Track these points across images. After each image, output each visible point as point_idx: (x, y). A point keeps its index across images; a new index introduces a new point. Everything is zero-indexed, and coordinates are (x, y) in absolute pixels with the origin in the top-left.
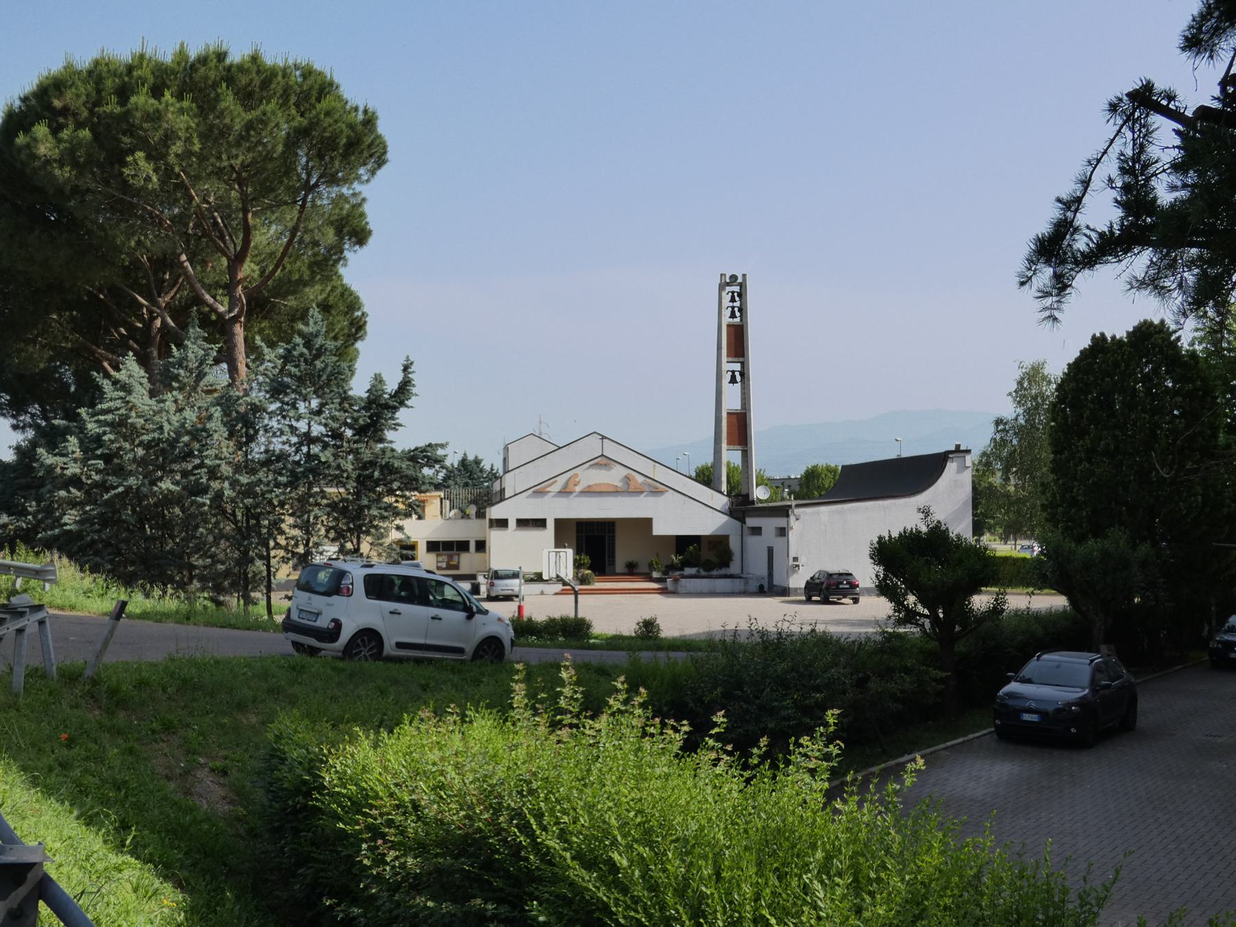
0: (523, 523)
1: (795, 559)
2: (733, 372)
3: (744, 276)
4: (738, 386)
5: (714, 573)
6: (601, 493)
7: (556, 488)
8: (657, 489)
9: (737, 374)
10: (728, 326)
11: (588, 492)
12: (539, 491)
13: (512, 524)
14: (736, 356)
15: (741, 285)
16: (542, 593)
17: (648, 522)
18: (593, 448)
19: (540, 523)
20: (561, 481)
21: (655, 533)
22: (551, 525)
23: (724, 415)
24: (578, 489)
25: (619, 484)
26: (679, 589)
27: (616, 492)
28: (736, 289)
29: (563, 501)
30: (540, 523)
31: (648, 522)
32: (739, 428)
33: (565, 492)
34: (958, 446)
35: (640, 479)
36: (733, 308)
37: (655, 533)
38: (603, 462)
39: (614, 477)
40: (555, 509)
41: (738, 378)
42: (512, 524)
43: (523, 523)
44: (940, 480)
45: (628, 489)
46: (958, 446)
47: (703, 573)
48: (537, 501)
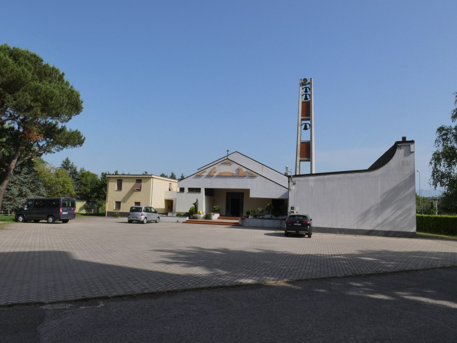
0: (191, 190)
1: (292, 208)
2: (306, 124)
3: (311, 79)
4: (309, 130)
5: (280, 218)
6: (226, 177)
7: (205, 174)
8: (252, 175)
9: (308, 125)
10: (303, 102)
11: (220, 176)
12: (198, 176)
13: (186, 190)
14: (306, 116)
15: (309, 83)
16: (178, 222)
17: (248, 191)
18: (226, 158)
19: (198, 190)
20: (208, 171)
21: (251, 196)
22: (203, 191)
23: (299, 143)
24: (215, 174)
25: (235, 172)
26: (244, 224)
27: (233, 176)
28: (305, 83)
29: (208, 180)
30: (198, 190)
31: (248, 191)
32: (306, 151)
33: (209, 176)
34: (404, 138)
35: (245, 170)
36: (306, 95)
37: (251, 196)
38: (227, 161)
39: (232, 169)
40: (205, 183)
41: (308, 127)
42: (186, 190)
43: (191, 190)
44: (391, 161)
45: (239, 175)
46: (404, 138)
47: (274, 217)
48: (198, 180)
